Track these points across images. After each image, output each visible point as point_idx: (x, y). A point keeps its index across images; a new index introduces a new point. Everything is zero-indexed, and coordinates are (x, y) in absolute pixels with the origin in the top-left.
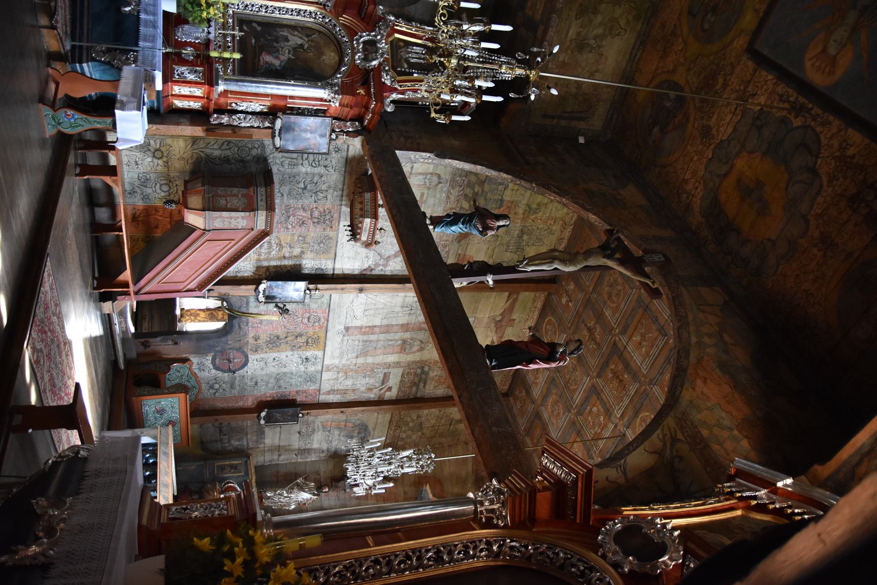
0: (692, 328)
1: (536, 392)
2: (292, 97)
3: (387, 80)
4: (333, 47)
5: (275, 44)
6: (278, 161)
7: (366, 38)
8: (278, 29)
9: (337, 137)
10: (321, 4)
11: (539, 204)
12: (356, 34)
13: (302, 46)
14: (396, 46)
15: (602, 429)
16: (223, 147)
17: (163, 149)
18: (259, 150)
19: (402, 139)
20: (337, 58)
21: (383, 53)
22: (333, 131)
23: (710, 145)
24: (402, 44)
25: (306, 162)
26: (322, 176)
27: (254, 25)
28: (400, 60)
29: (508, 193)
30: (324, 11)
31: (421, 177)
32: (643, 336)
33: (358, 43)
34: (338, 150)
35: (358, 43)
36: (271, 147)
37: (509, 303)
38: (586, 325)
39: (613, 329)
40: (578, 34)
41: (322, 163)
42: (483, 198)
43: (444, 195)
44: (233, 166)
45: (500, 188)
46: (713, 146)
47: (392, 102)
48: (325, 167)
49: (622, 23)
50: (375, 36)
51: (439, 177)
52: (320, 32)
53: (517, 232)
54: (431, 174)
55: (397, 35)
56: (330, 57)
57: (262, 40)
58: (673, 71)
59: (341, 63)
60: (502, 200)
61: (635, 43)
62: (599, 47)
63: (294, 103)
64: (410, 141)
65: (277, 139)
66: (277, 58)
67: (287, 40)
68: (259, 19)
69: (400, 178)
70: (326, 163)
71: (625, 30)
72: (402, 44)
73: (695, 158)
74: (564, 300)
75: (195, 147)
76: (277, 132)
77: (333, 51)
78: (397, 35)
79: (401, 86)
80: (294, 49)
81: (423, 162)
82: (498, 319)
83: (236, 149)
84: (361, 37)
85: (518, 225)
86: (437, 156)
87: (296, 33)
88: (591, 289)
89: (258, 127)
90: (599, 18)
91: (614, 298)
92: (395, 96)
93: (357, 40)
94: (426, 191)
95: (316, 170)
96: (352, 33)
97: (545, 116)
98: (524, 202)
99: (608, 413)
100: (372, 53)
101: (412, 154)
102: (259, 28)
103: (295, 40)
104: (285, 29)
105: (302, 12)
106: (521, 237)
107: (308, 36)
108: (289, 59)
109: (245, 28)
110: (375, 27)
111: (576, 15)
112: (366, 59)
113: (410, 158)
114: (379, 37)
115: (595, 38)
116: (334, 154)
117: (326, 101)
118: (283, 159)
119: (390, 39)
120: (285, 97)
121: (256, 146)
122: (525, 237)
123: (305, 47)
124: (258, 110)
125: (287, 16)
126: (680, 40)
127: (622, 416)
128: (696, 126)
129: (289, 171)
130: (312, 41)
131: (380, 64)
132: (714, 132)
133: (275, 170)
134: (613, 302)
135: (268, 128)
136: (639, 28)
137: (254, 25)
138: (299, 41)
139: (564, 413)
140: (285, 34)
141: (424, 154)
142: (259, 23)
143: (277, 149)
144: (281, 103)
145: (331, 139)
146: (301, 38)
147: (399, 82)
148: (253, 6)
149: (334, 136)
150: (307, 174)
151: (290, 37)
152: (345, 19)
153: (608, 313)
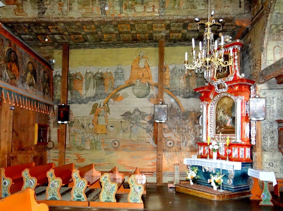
2: (242, 115)
3: (231, 78)
4: (222, 100)
5: (223, 121)
6: (272, 117)
7: (217, 88)
8: (218, 120)
9: (258, 95)
10: (207, 106)
12: (216, 92)
13: (223, 111)
14: (219, 77)
16: (267, 140)
17: (269, 163)
18: (267, 125)
19: (257, 68)
20: (226, 98)
21: (222, 81)
22: (255, 97)
24: (218, 75)
25: (271, 106)
26: (278, 99)
27: (217, 128)
28: (224, 74)
30: (209, 105)
31: (276, 55)
33: (219, 91)
34: (265, 94)
35: (219, 91)
36: (265, 120)
41: (271, 99)
44: (275, 136)
47: (240, 75)
48: (273, 98)
50: (216, 85)
51: (275, 47)
52: (217, 105)
54: (274, 51)
55: (215, 77)
56: (226, 101)
57: (222, 126)
63: (244, 113)
64: (257, 64)
65: (260, 119)
66: (228, 120)
67: (221, 117)
68: (215, 127)
69: (273, 66)
70: (271, 98)
75: (267, 150)
76: (258, 119)
77: (224, 100)
78: (215, 77)
79: (234, 72)
80: (224, 114)
81: (266, 57)
83: (267, 134)
84: (217, 90)
86: (262, 51)
87: (218, 114)
89: (256, 126)
92: (238, 74)
95: (275, 102)
96: (216, 94)
97: (240, 7)
101: (263, 62)
102: (218, 127)
103: (221, 114)
104: (217, 118)
105: (211, 112)
107: (219, 110)
108: (228, 116)
109: (218, 132)
110: (212, 86)
111: (195, 8)
112: (225, 88)
113: (265, 63)
114: (216, 84)
116: (267, 95)
117: (242, 101)
118: (270, 115)
119: (216, 79)
120: (242, 117)
121: (265, 126)
123: (223, 110)
124: (249, 127)
125: (213, 117)
129: (276, 113)
130: (221, 108)
131: (226, 82)
133: (276, 119)
135: (255, 122)
137: (217, 128)
138: (221, 112)
140: (219, 118)
141: (262, 57)
142: (216, 127)
143: (265, 119)
144: (244, 118)
145: (259, 97)
146: (220, 112)
147: (232, 73)
148: (210, 129)
149: (257, 96)
150: (277, 105)
151: (220, 116)
152: (211, 96)
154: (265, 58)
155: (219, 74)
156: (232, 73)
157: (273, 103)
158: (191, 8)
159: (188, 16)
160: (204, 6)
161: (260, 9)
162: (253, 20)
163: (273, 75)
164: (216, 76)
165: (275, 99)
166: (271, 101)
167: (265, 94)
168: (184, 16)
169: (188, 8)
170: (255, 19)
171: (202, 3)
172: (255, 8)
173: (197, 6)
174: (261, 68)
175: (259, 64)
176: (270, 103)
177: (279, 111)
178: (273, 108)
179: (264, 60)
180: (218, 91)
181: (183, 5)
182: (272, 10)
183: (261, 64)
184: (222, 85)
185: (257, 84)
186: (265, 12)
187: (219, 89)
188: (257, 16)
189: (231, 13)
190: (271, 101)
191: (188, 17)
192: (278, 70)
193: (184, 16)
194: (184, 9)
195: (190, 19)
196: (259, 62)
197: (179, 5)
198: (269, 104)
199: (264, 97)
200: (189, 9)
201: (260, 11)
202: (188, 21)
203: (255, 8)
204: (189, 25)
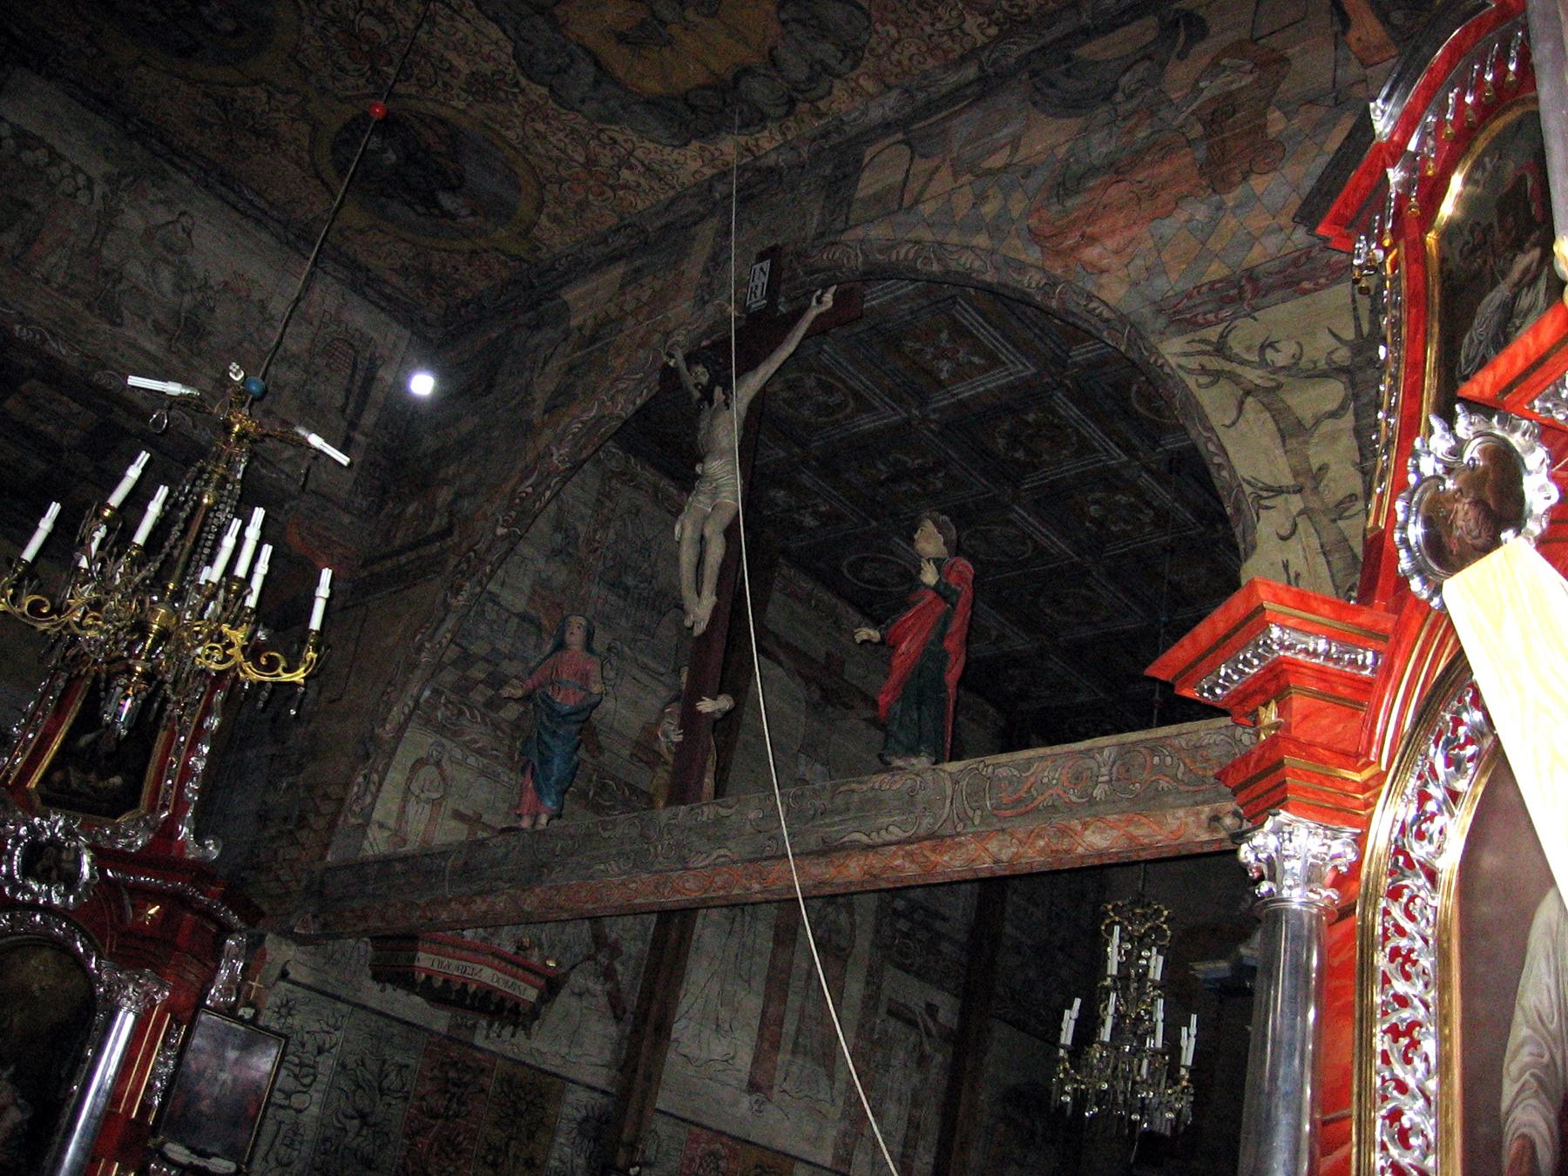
0: (954, 237)
1: (1020, 643)
11: (558, 527)
15: (1149, 505)
19: (303, 835)
23: (517, 84)
25: (296, 1101)
26: (344, 1066)
28: (95, 789)
29: (507, 597)
31: (412, 809)
32: (941, 354)
34: (287, 1008)
37: (782, 657)
38: (882, 484)
39: (908, 422)
40: (159, 329)
41: (308, 1059)
42: (505, 663)
43: (471, 760)
45: (491, 612)
46: (524, 82)
47: (199, 835)
48: (320, 1051)
49: (161, 215)
50: (18, 839)
51: (420, 763)
53: (612, 598)
54: (409, 780)
55: (33, 783)
58: (316, 126)
59: (62, 948)
60: (523, 617)
61: (221, 197)
62: (205, 286)
64: (312, 818)
71: (182, 214)
72: (58, 776)
73: (541, 127)
74: (809, 521)
78: (33, 783)
79: (164, 807)
81: (375, 797)
82: (816, 696)
85: (595, 591)
88: (797, 450)
90: (135, 269)
91: (835, 399)
93: (16, 888)
94: (450, 803)
98: (541, 564)
99: (1109, 480)
100: (58, 861)
106: (627, 589)
111: (113, 323)
115: (179, 289)
116: (296, 1021)
118: (271, 1157)
119: (37, 802)
122: (630, 581)
126: (242, 91)
127: (1129, 449)
128: (462, 105)
132: (487, 68)
134: (841, 406)
136: (185, 180)
139: (1089, 588)
149: (246, 1013)
150: (325, 1105)
153: (866, 423)
154: (368, 799)
155: (67, 774)
156: (152, 809)
157: (307, 1081)
158: (89, 306)
159: (53, 335)
160: (162, 340)
161: (432, 529)
162: (377, 568)
163: (383, 918)
164: (44, 780)
165: (326, 1064)
166: (305, 1070)
167: (283, 1011)
168: (25, 321)
169: (74, 295)
170: (388, 564)
171: (161, 318)
172: (411, 509)
173: (126, 313)
174: (326, 846)
175: (321, 823)
176: (296, 1077)
177: (326, 1140)
178: (299, 1111)
179: (357, 809)
180: (16, 888)
181: (53, 260)
182: (488, 569)
183: (331, 826)
184: (64, 856)
185: (270, 936)
186: (453, 561)
187: (27, 870)
188: (403, 559)
189: (287, 468)
190: (301, 1065)
191: (44, 341)
192: (422, 902)
193: (25, 321)
194: (47, 281)
195: (50, 358)
196: (327, 808)
197: (28, 243)
198: (290, 1084)
199: (274, 1026)
200: (74, 304)
201: (428, 541)
202: (29, 362)
203: (411, 509)
204: (23, 387)
